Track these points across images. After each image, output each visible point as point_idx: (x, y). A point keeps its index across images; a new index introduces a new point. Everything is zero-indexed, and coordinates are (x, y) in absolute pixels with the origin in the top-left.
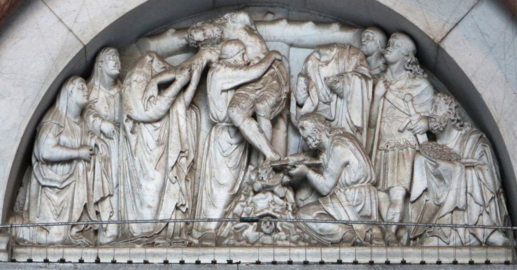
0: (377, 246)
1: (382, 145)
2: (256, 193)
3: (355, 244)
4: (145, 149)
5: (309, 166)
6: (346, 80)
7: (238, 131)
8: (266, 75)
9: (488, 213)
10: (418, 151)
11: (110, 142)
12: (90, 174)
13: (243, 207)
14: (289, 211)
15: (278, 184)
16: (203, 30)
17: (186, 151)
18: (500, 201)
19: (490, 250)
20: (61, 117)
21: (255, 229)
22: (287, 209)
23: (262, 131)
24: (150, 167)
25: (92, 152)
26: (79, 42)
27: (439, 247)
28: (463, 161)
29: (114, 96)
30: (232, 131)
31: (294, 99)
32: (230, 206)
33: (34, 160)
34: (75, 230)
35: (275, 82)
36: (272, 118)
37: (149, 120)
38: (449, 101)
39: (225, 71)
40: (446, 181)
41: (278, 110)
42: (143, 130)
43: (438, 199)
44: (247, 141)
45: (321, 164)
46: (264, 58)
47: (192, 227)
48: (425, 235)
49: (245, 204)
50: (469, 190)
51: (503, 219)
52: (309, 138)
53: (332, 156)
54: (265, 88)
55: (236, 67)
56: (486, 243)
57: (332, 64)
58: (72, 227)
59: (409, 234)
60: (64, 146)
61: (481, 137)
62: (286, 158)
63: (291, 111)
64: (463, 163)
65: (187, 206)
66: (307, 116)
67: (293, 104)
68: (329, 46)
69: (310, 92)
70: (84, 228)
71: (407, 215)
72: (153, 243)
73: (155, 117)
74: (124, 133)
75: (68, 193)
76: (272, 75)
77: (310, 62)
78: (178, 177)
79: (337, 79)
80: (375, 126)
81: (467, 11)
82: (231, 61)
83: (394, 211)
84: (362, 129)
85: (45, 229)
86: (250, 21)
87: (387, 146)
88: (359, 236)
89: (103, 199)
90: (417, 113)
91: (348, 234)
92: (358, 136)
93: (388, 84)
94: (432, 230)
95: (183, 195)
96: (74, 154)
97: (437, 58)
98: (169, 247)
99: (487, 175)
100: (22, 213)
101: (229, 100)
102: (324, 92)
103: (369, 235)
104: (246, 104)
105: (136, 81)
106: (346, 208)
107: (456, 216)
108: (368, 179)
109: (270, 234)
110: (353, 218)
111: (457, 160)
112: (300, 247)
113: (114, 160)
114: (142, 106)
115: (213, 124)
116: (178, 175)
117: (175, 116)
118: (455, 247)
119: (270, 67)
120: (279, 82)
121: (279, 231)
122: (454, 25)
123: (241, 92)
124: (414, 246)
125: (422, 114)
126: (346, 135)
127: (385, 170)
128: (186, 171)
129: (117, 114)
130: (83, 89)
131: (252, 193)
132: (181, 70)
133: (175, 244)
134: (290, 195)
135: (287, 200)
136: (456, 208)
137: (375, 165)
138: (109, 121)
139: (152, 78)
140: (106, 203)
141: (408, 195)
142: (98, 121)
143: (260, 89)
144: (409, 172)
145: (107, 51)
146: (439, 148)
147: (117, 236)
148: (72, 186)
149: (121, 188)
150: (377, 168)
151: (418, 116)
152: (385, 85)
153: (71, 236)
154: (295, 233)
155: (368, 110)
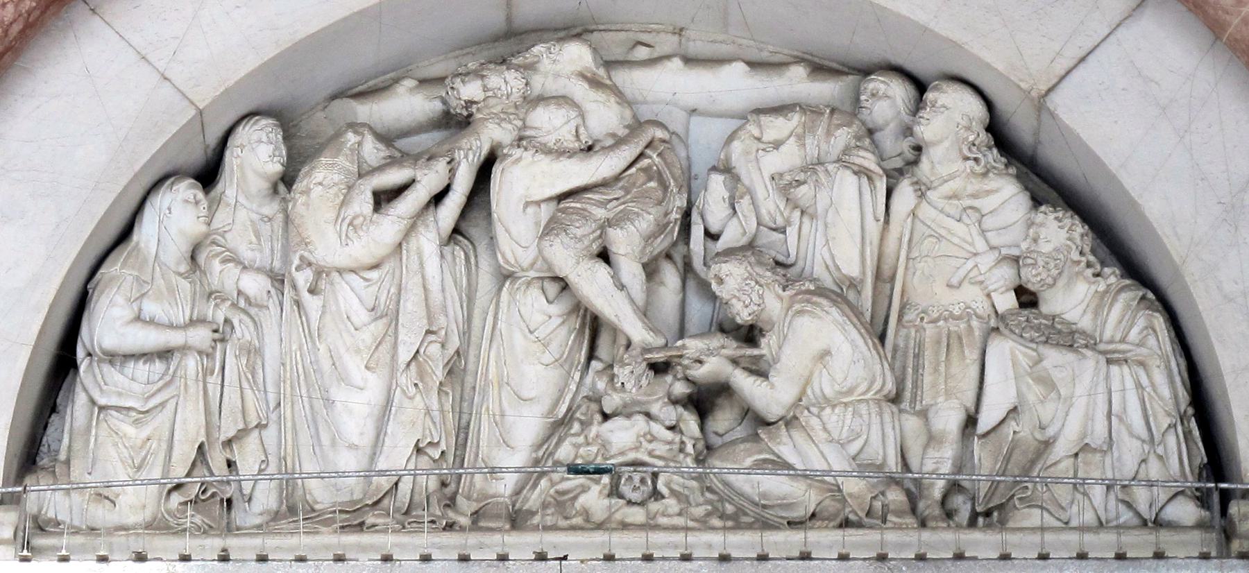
0: (898, 527)
2: (606, 417)
3: (846, 524)
4: (342, 326)
5: (735, 362)
6: (822, 175)
7: (564, 285)
8: (633, 170)
9: (1160, 457)
10: (997, 329)
11: (261, 314)
12: (214, 380)
14: (687, 455)
15: (659, 398)
16: (483, 77)
17: (440, 329)
18: (1187, 434)
19: (1165, 536)
20: (145, 261)
21: (606, 492)
22: (681, 450)
23: (622, 287)
24: (354, 366)
25: (216, 336)
26: (186, 103)
27: (1043, 529)
28: (1102, 347)
29: (270, 220)
30: (552, 288)
31: (700, 221)
32: (545, 447)
33: (80, 353)
34: (176, 498)
35: (653, 184)
36: (645, 260)
37: (353, 265)
38: (1068, 222)
39: (534, 162)
40: (1063, 392)
41: (661, 244)
42: (338, 287)
43: (1042, 428)
44: (586, 310)
45: (762, 356)
46: (628, 136)
47: (456, 493)
48: (1011, 503)
49: (581, 439)
50: (1115, 408)
51: (1197, 471)
52: (734, 301)
53: (790, 336)
54: (629, 197)
55: (560, 153)
56: (1155, 522)
57: (791, 146)
58: (170, 492)
59: (973, 505)
60: (152, 322)
61: (1143, 298)
62: (679, 343)
63: (692, 246)
64: (1103, 353)
65: (443, 446)
66: (729, 253)
68: (780, 109)
69: (737, 206)
70: (197, 496)
71: (969, 465)
72: (362, 524)
73: (370, 261)
74: (292, 293)
75: (162, 419)
76: (646, 170)
77: (736, 145)
78: (420, 385)
79: (802, 177)
80: (892, 279)
81: (1106, 32)
82: (550, 140)
83: (937, 455)
84: (862, 281)
85: (107, 498)
86: (595, 60)
87: (922, 319)
88: (856, 508)
89: (242, 434)
90: (992, 248)
91: (827, 502)
92: (851, 296)
93: (923, 188)
94: (1029, 493)
95: (434, 423)
96: (174, 338)
97: (1037, 133)
98: (399, 531)
99: (1160, 378)
100: (54, 466)
101: (543, 224)
102: (772, 208)
103: (878, 505)
104: (583, 230)
105: (320, 184)
106: (823, 447)
107: (1085, 463)
108: (877, 386)
109: (641, 504)
111: (1086, 346)
112: (713, 529)
113: (271, 351)
114: (336, 236)
115: (505, 276)
116: (422, 381)
117: (414, 258)
118: (1082, 529)
119: (641, 155)
120: (664, 186)
121: (663, 497)
122: (1075, 61)
123: (573, 205)
124: (989, 526)
125: (1004, 251)
126: (821, 292)
127: (916, 370)
128: (440, 374)
129: (278, 255)
130: (197, 203)
131: (598, 417)
132: (429, 159)
133: (414, 525)
134: (691, 423)
135: (681, 432)
136: (1086, 448)
137: (893, 357)
139: (360, 176)
140: (252, 440)
141: (971, 421)
142: (232, 270)
143: (617, 199)
144: (974, 372)
145: (255, 123)
146: (1044, 321)
147: (277, 513)
148: (171, 406)
149: (286, 410)
150: (898, 364)
151: (993, 256)
152: (916, 191)
153: (169, 512)
154: (701, 500)
155: (876, 241)
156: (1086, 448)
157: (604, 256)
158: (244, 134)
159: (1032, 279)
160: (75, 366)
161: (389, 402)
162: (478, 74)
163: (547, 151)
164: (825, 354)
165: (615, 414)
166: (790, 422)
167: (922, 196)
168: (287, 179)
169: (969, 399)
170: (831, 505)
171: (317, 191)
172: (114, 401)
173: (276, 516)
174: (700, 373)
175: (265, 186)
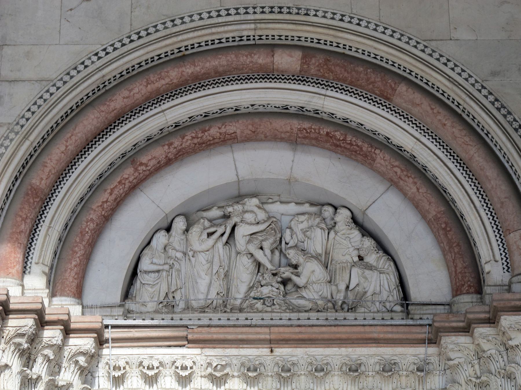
0: (331, 312)
1: (333, 262)
2: (262, 286)
3: (318, 311)
5: (292, 273)
7: (252, 255)
10: (354, 266)
12: (170, 277)
13: (255, 293)
18: (399, 290)
19: (393, 314)
23: (266, 256)
24: (203, 274)
27: (364, 312)
28: (379, 270)
30: (249, 256)
33: (138, 271)
34: (161, 305)
37: (202, 250)
38: (370, 240)
41: (275, 245)
43: (364, 289)
50: (382, 284)
55: (251, 224)
57: (305, 222)
60: (155, 264)
67: (283, 243)
68: (303, 214)
73: (206, 249)
75: (157, 287)
76: (271, 228)
77: (292, 222)
79: (308, 230)
80: (329, 254)
82: (249, 221)
92: (320, 258)
96: (161, 268)
99: (392, 277)
103: (326, 307)
104: (256, 242)
108: (326, 279)
109: (270, 306)
110: (316, 297)
112: (287, 312)
113: (183, 271)
115: (238, 253)
117: (217, 249)
118: (374, 312)
119: (270, 225)
120: (276, 232)
124: (352, 312)
127: (335, 275)
128: (223, 276)
129: (185, 248)
131: (260, 286)
134: (282, 287)
136: (375, 293)
138: (180, 252)
139: (204, 229)
141: (348, 287)
142: (174, 251)
144: (348, 275)
149: (187, 284)
156: (375, 293)
157: (261, 248)
158: (177, 220)
159: (362, 253)
160: (137, 274)
161: (211, 282)
162: (232, 206)
163: (248, 224)
164: (313, 271)
165: (264, 285)
166: (305, 287)
167: (336, 234)
168: (187, 230)
169: (348, 283)
170: (315, 307)
171: (194, 233)
172: (146, 282)
173: (184, 309)
174: (284, 276)
175: (182, 232)
